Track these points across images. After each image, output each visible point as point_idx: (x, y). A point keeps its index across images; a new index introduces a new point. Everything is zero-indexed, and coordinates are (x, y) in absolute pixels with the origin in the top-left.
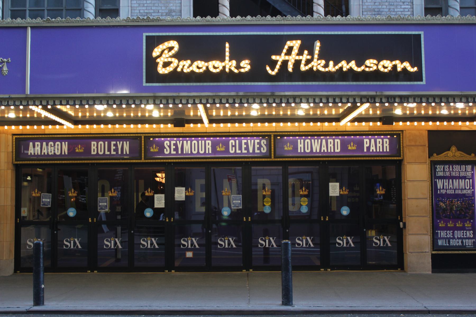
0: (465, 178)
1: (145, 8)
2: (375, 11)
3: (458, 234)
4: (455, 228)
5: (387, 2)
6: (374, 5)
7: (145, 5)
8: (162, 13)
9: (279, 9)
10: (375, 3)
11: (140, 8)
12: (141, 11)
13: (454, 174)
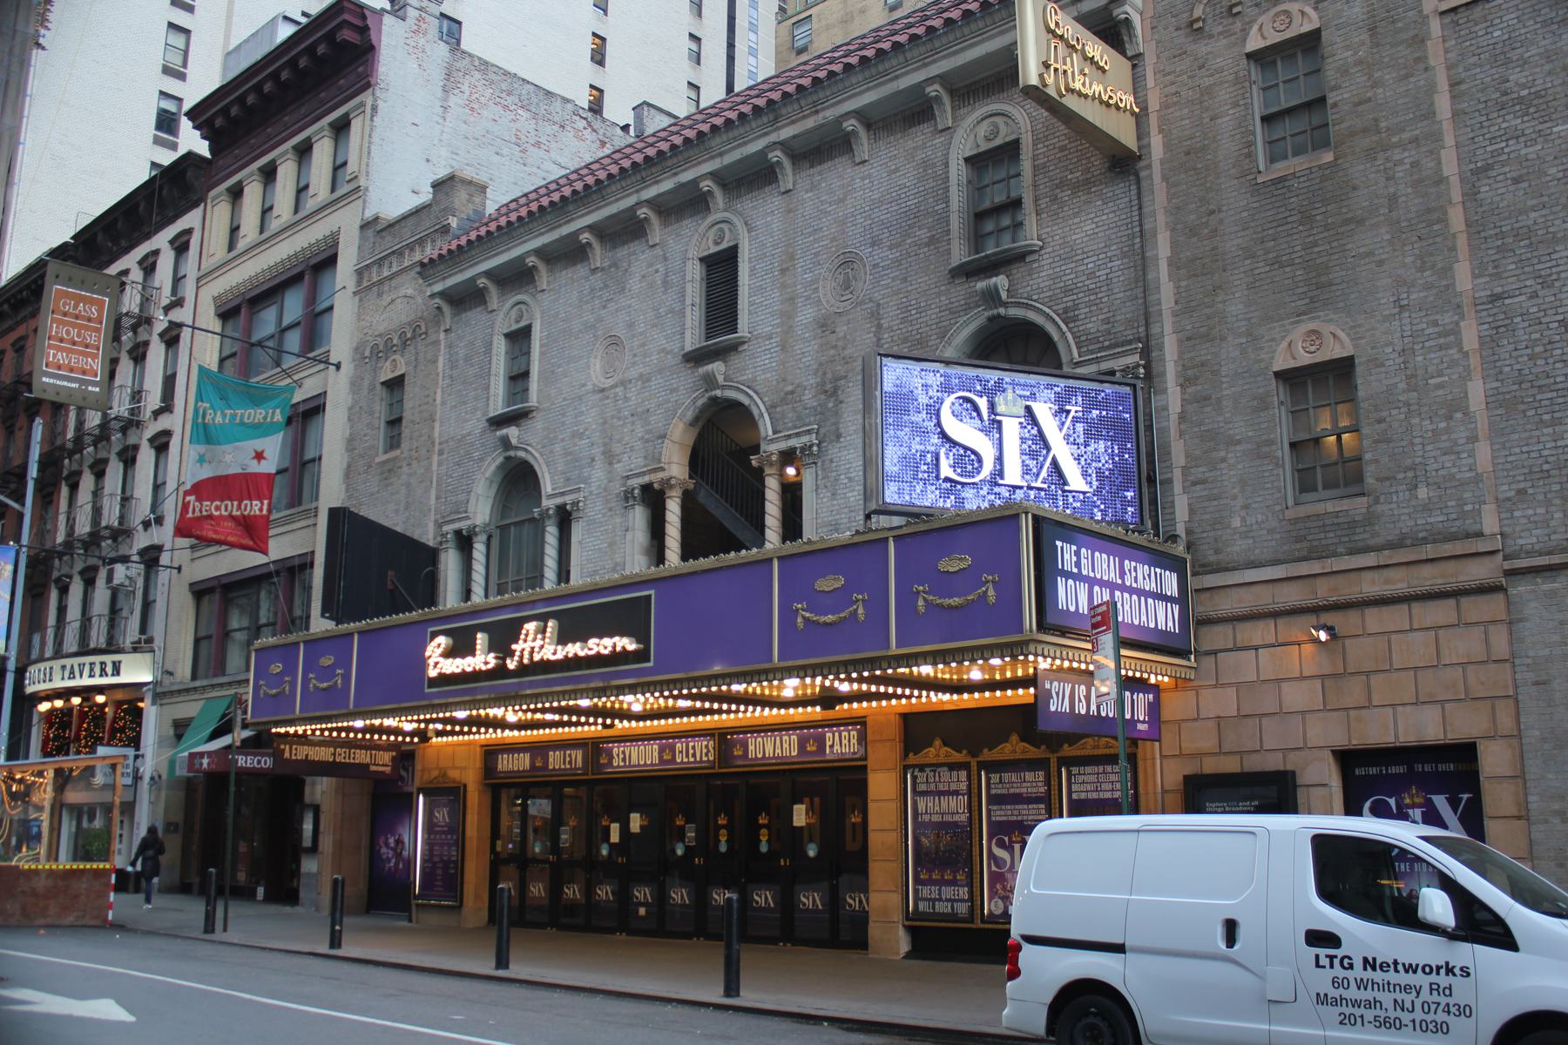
0: (956, 793)
3: (948, 892)
4: (942, 883)
13: (941, 787)
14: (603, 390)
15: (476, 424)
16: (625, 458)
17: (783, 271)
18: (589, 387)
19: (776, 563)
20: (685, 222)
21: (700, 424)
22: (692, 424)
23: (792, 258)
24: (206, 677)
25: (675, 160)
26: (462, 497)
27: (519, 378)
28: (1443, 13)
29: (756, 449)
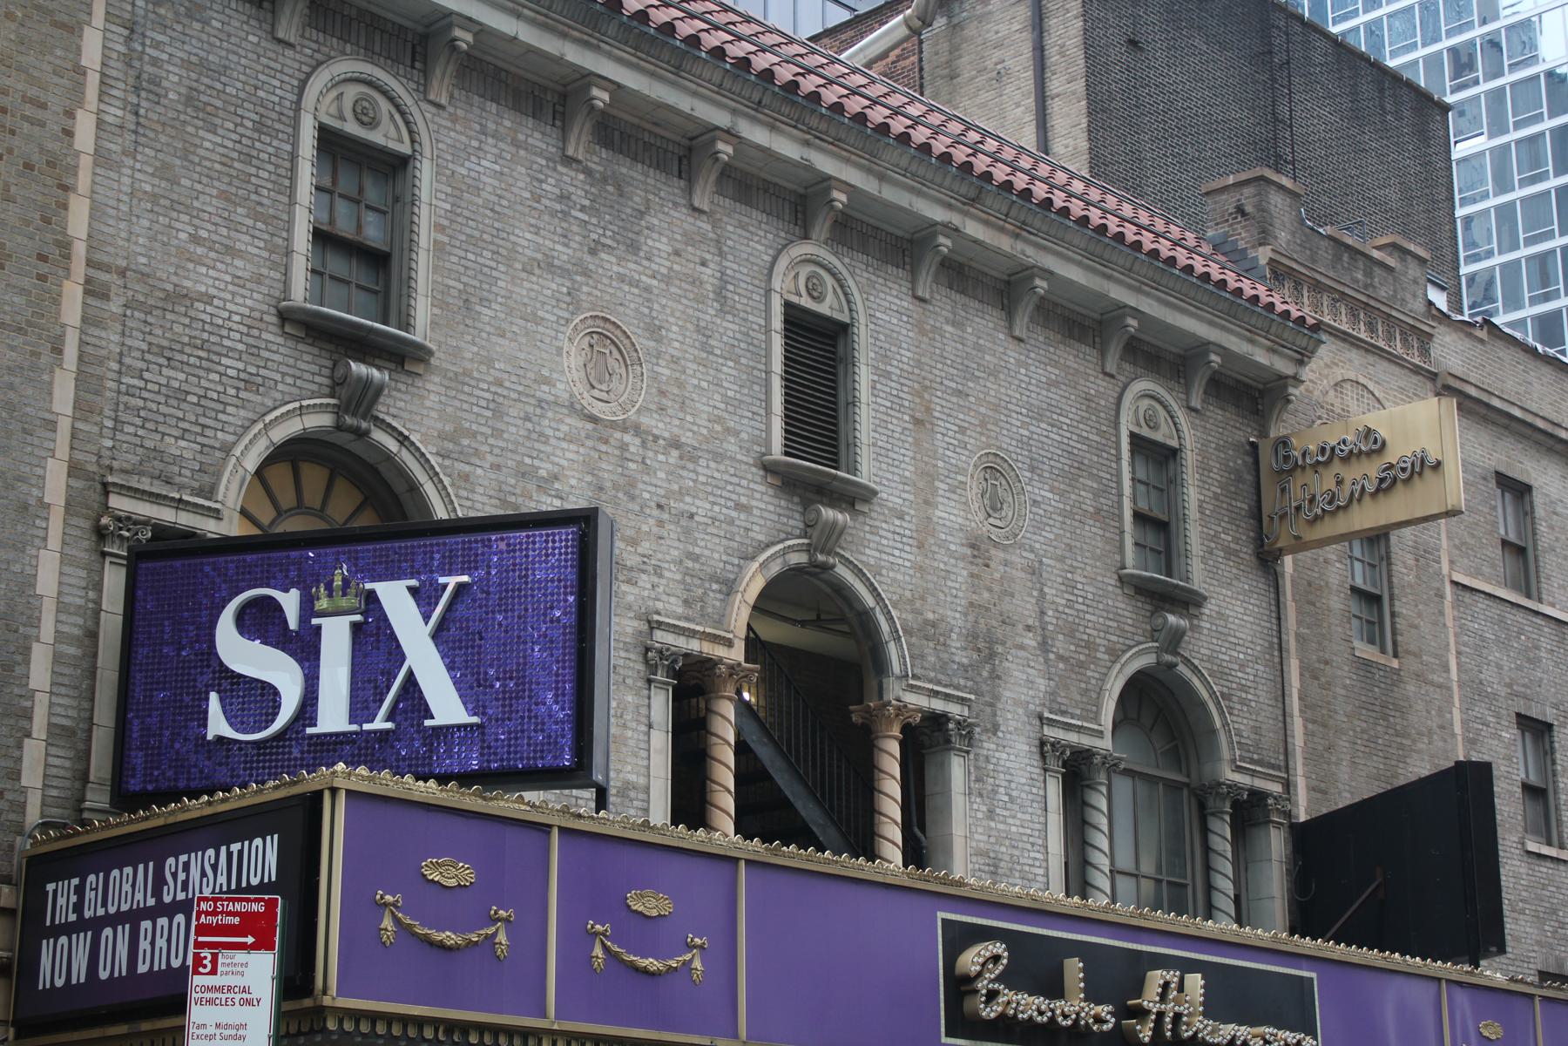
14: (593, 419)
17: (918, 422)
20: (754, 213)
23: (929, 410)
25: (823, 126)
28: (1455, 583)
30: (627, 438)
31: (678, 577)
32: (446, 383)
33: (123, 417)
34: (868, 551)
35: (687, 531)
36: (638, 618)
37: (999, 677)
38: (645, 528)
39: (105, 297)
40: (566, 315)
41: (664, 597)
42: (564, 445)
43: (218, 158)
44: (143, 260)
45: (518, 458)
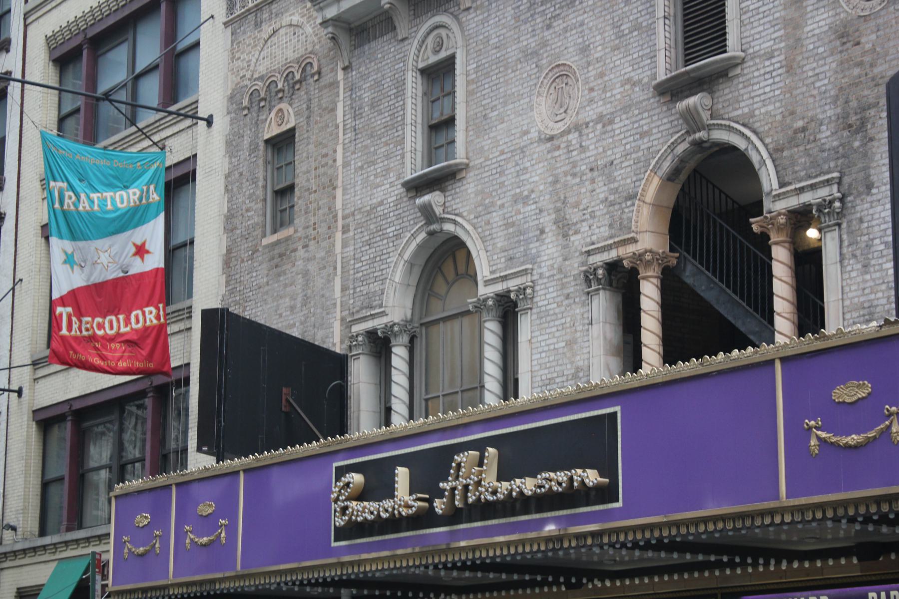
1: (546, 371)
2: (864, 308)
5: (884, 282)
6: (863, 295)
7: (548, 365)
8: (567, 375)
9: (742, 329)
10: (864, 289)
11: (542, 372)
12: (544, 378)
14: (551, 138)
15: (390, 191)
16: (584, 227)
18: (534, 135)
19: (778, 365)
21: (683, 177)
22: (672, 177)
24: (58, 531)
26: (375, 287)
27: (440, 127)
29: (757, 208)
30: (570, 137)
31: (605, 211)
32: (476, 172)
33: (356, 285)
34: (742, 104)
35: (611, 179)
36: (582, 253)
37: (871, 139)
38: (583, 190)
39: (349, 230)
40: (535, 81)
41: (597, 231)
42: (536, 167)
43: (382, 126)
44: (359, 202)
45: (513, 193)
